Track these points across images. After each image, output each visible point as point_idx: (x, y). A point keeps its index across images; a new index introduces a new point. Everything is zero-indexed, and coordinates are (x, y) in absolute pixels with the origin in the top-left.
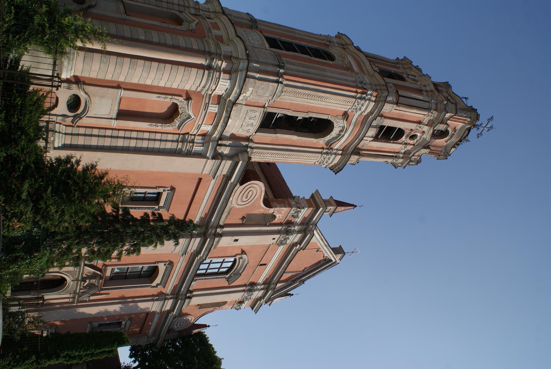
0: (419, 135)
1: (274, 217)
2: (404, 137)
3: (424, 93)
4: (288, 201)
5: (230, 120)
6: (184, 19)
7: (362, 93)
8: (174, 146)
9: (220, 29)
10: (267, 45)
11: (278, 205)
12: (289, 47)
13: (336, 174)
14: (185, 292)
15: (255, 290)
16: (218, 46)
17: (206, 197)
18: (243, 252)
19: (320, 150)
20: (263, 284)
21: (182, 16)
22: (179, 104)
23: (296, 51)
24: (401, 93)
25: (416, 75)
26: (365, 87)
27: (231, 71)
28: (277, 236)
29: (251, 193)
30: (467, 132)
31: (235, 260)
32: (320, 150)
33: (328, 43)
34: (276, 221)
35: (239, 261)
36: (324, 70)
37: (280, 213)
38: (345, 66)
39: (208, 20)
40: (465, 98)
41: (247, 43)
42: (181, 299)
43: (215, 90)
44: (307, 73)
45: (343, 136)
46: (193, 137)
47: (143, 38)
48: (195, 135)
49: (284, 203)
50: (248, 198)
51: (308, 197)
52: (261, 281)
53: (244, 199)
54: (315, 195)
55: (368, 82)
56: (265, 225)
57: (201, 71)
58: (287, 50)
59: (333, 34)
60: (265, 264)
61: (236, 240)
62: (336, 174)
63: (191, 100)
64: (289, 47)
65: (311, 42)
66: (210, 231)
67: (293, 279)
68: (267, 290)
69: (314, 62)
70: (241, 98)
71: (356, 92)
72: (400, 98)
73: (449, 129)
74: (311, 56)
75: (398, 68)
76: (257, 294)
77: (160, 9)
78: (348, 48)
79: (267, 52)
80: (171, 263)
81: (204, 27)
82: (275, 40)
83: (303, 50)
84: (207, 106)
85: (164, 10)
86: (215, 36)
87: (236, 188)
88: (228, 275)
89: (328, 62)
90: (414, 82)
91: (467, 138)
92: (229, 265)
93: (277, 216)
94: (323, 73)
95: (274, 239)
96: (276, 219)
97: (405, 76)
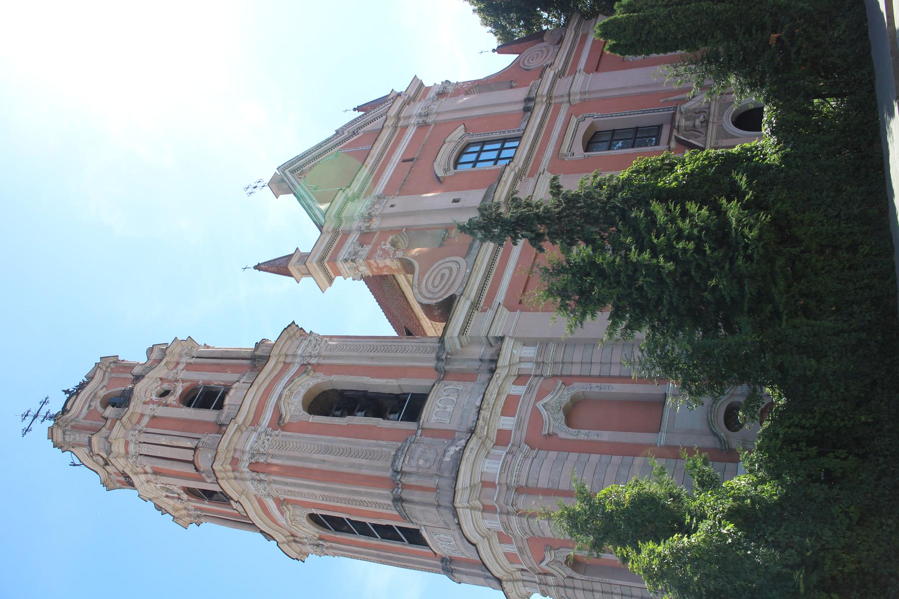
2: (179, 391)
3: (149, 470)
4: (372, 271)
5: (478, 404)
6: (564, 566)
9: (505, 553)
10: (424, 534)
12: (387, 532)
13: (293, 322)
15: (420, 115)
16: (507, 527)
21: (569, 571)
22: (566, 427)
23: (374, 526)
24: (190, 469)
25: (167, 500)
26: (254, 474)
27: (483, 486)
30: (68, 407)
31: (455, 168)
33: (321, 542)
35: (449, 165)
36: (324, 498)
37: (384, 250)
38: (290, 506)
39: (525, 568)
40: (75, 465)
41: (457, 533)
42: (542, 96)
43: (507, 453)
45: (285, 388)
48: (536, 376)
50: (440, 274)
51: (338, 280)
54: (327, 283)
55: (249, 483)
57: (531, 483)
58: (389, 528)
59: (312, 559)
60: (404, 161)
61: (455, 201)
62: (293, 322)
63: (545, 435)
64: (387, 532)
65: (350, 543)
67: (355, 137)
68: (398, 117)
69: (343, 510)
70: (463, 442)
72: (191, 459)
73: (100, 409)
74: (348, 519)
75: (196, 509)
76: (417, 108)
77: (608, 580)
78: (286, 537)
79: (424, 523)
81: (530, 555)
82: (411, 542)
83: (363, 529)
84: (519, 425)
85: (597, 579)
86: (511, 543)
87: (461, 289)
88: (467, 139)
89: (319, 512)
90: (168, 486)
91: (68, 395)
92: (465, 158)
93: (388, 246)
94: (327, 493)
95: (392, 206)
96: (389, 240)
97: (185, 496)
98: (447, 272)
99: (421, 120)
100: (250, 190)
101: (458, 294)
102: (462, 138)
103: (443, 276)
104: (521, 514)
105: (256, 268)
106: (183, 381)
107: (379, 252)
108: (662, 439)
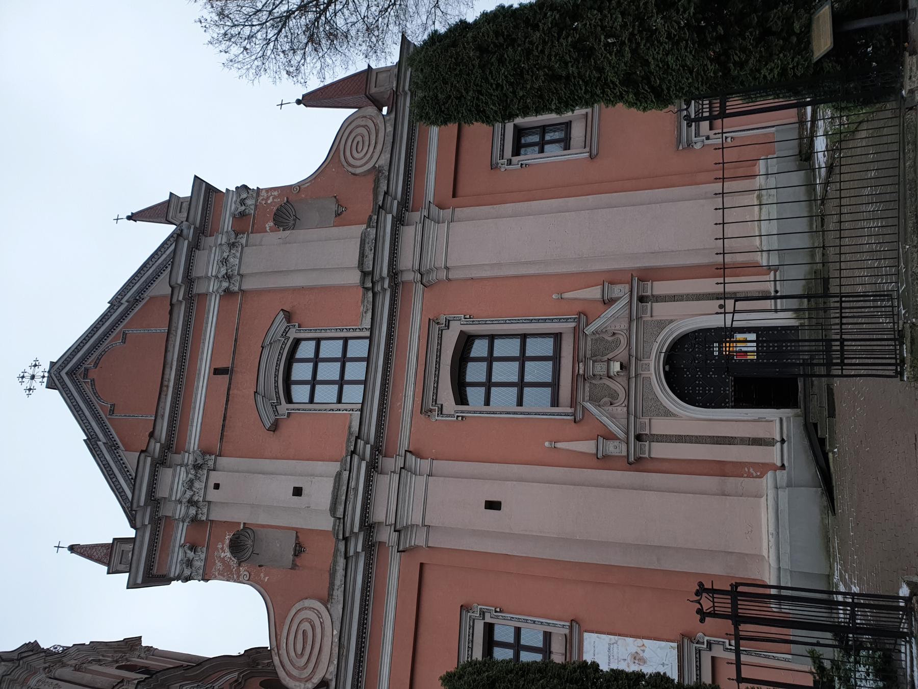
14: (379, 299)
17: (388, 648)
18: (275, 427)
29: (299, 651)
35: (278, 398)
37: (222, 560)
42: (382, 279)
52: (214, 305)
53: (306, 626)
66: (359, 549)
67: (141, 305)
80: (425, 411)
87: (333, 668)
88: (293, 334)
93: (228, 554)
100: (27, 383)
101: (331, 676)
102: (286, 332)
103: (304, 632)
107: (219, 565)
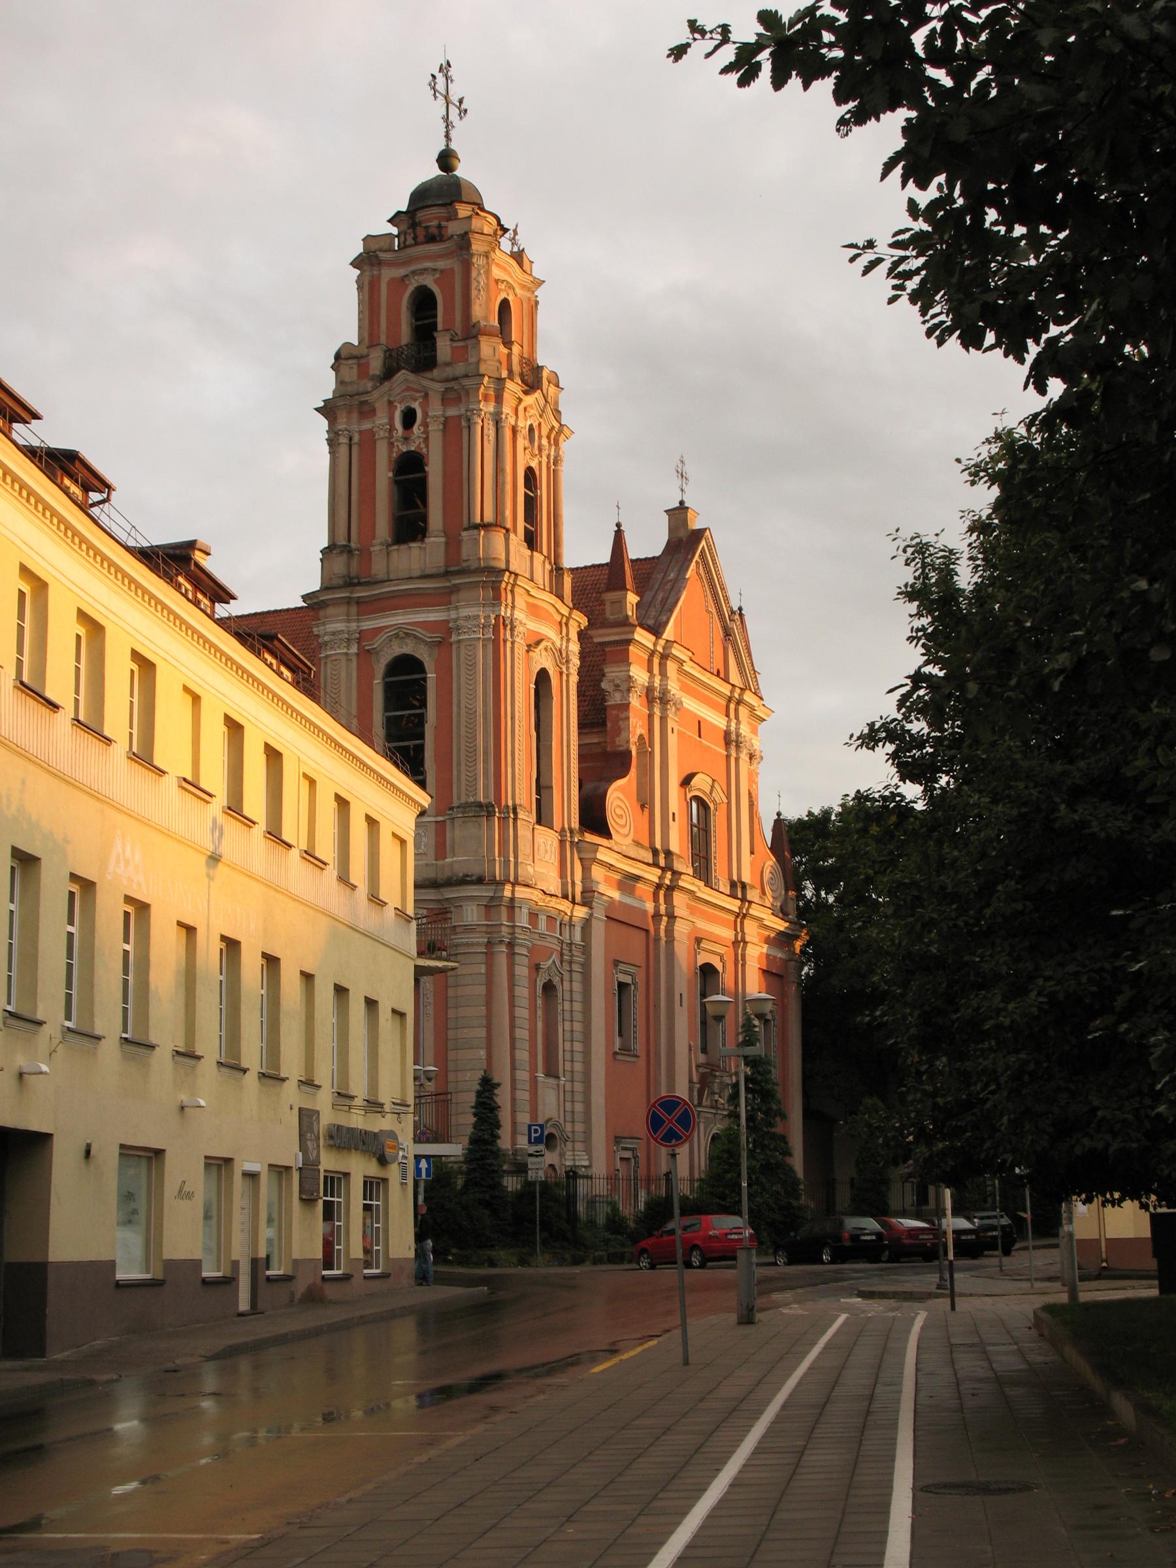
0: (529, 423)
1: (641, 736)
2: (534, 464)
7: (505, 626)
8: (577, 977)
11: (624, 734)
15: (738, 735)
16: (469, 929)
19: (564, 677)
20: (727, 715)
28: (671, 724)
32: (564, 677)
34: (644, 732)
44: (486, 754)
46: (564, 946)
47: (483, 1053)
49: (617, 719)
56: (652, 753)
71: (505, 641)
84: (542, 936)
88: (712, 806)
98: (622, 822)
99: (733, 737)
102: (714, 801)
104: (489, 944)
105: (618, 525)
106: (540, 463)
108: (540, 1074)
